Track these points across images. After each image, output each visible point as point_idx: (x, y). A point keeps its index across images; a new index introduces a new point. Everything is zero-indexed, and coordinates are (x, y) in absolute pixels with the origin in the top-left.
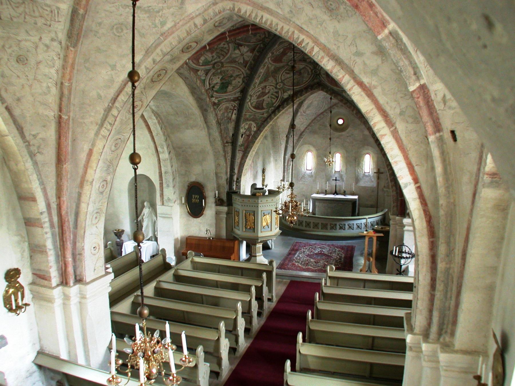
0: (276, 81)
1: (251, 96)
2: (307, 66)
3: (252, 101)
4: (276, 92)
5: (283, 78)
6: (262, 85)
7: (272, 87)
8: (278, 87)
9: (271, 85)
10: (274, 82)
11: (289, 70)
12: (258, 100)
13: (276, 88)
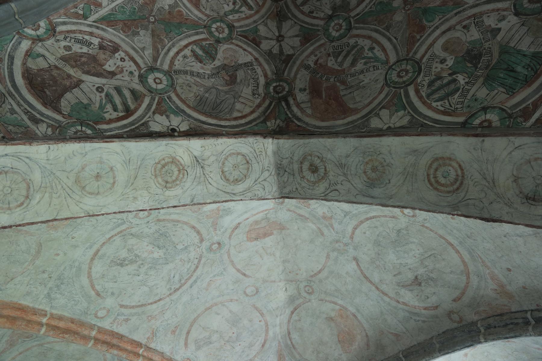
0: (155, 59)
1: (52, 31)
2: (260, 65)
3: (39, 49)
4: (133, 92)
5: (178, 65)
6: (111, 34)
7: (134, 68)
8: (150, 80)
9: (132, 59)
10: (148, 53)
11: (202, 48)
12: (61, 64)
13: (142, 79)
